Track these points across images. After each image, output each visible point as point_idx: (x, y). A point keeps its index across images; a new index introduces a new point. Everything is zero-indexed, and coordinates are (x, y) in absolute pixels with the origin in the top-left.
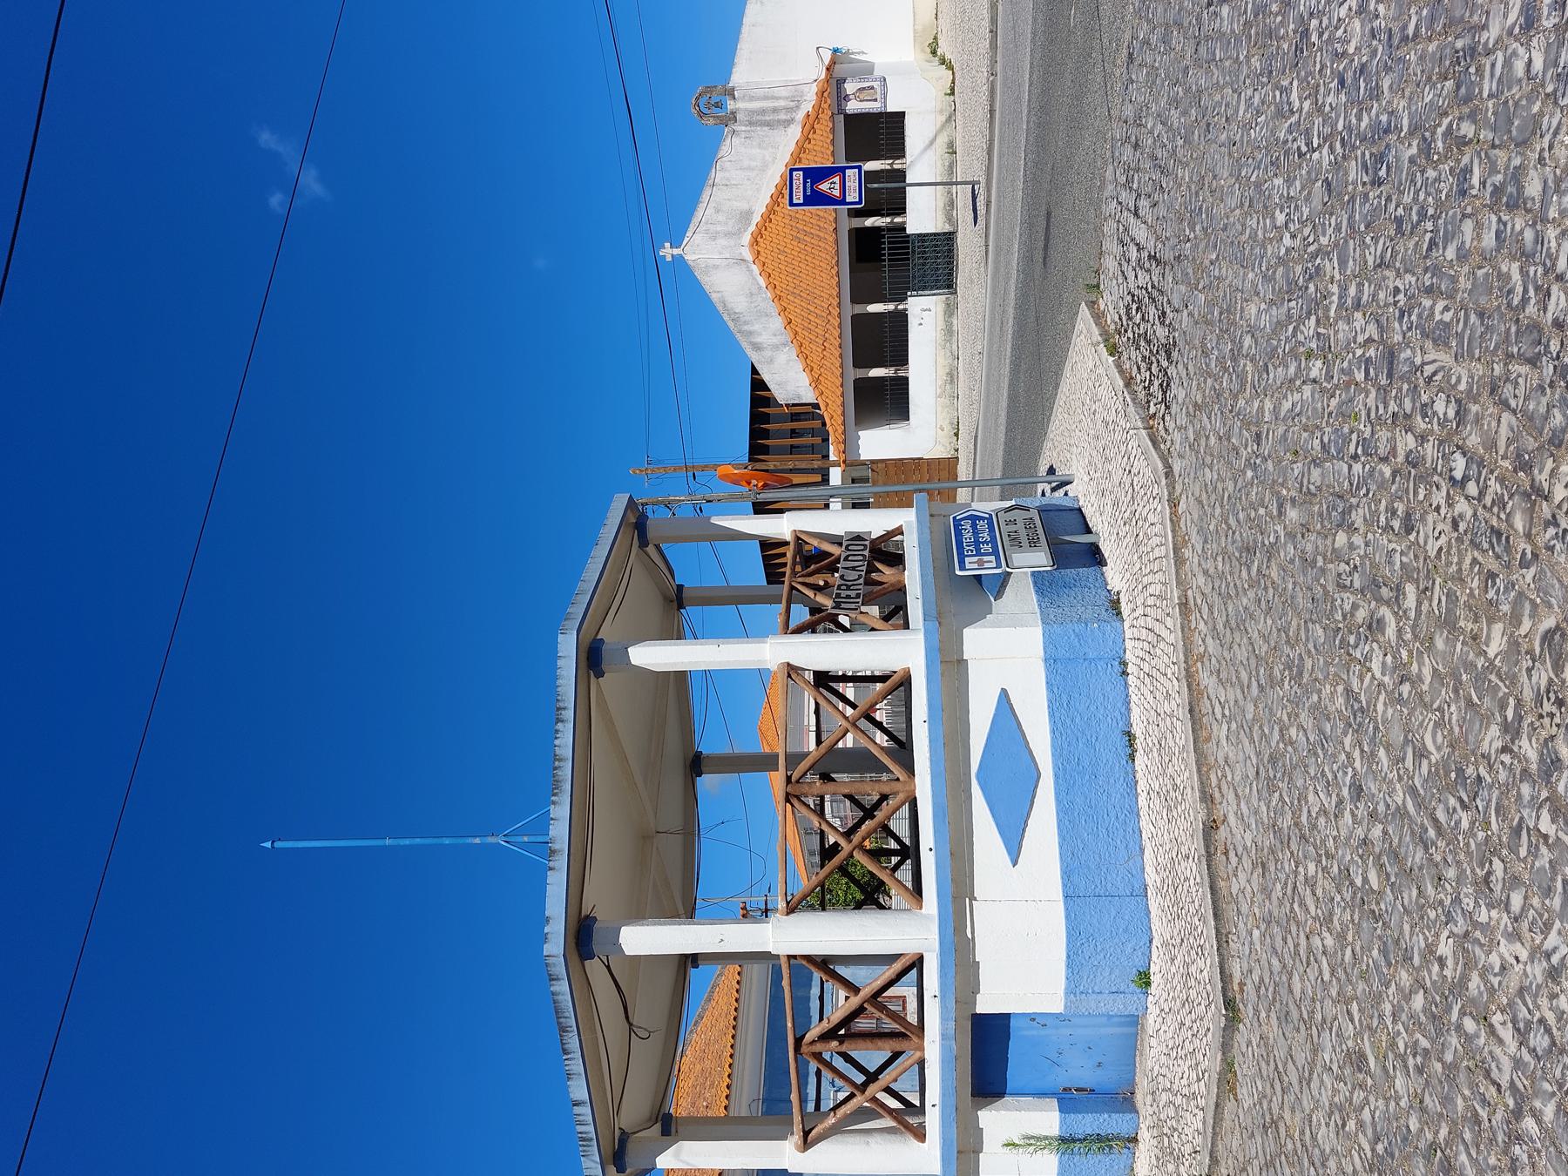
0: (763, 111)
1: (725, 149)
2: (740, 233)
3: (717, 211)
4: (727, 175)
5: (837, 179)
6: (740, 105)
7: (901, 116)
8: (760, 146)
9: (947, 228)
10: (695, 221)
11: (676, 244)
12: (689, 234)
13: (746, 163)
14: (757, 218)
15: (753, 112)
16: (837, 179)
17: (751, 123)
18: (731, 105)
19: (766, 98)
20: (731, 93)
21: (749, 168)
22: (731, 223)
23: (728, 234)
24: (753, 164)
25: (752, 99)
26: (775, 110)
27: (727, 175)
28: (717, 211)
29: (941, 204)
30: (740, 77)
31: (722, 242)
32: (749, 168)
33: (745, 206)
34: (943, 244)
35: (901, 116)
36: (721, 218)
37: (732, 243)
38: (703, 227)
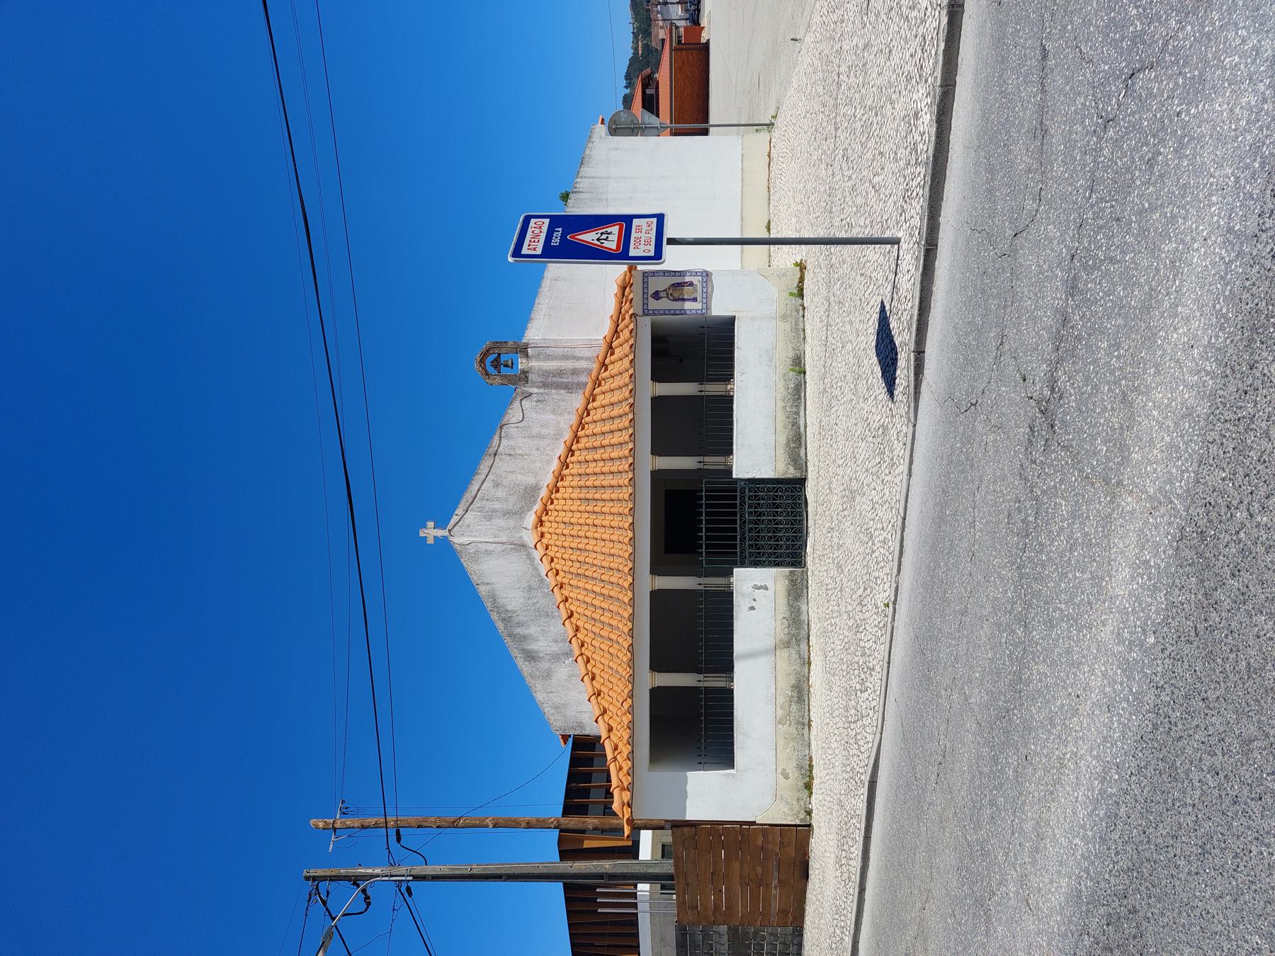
0: (560, 373)
1: (514, 414)
2: (520, 513)
3: (497, 485)
4: (512, 443)
5: (615, 229)
6: (534, 364)
7: (728, 325)
8: (554, 412)
9: (792, 473)
10: (468, 496)
11: (441, 524)
12: (459, 511)
13: (535, 431)
14: (544, 493)
15: (547, 373)
16: (615, 229)
17: (545, 385)
18: (522, 364)
19: (565, 357)
20: (523, 350)
21: (540, 436)
22: (512, 500)
23: (507, 514)
24: (545, 431)
25: (549, 358)
26: (575, 372)
27: (512, 443)
28: (497, 485)
29: (782, 439)
30: (534, 334)
31: (499, 522)
32: (540, 436)
33: (530, 480)
34: (786, 496)
35: (728, 325)
36: (500, 493)
37: (511, 523)
38: (477, 504)
